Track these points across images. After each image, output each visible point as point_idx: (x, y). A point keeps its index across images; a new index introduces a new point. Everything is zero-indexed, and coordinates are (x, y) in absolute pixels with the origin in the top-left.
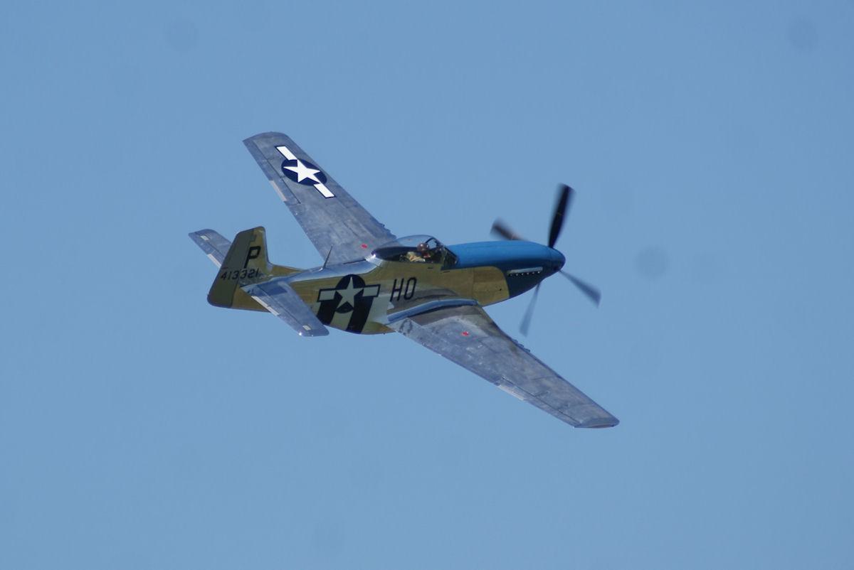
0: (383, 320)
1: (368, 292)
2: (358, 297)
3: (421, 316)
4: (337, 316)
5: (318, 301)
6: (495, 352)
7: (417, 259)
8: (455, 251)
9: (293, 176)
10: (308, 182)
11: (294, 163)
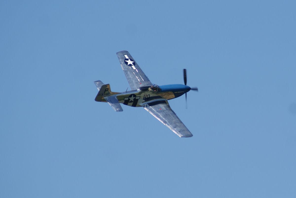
0: (141, 104)
1: (137, 98)
2: (135, 99)
3: (151, 104)
4: (129, 103)
5: (124, 100)
6: (166, 115)
7: (151, 90)
8: (161, 88)
9: (127, 63)
10: (130, 65)
11: (128, 60)
